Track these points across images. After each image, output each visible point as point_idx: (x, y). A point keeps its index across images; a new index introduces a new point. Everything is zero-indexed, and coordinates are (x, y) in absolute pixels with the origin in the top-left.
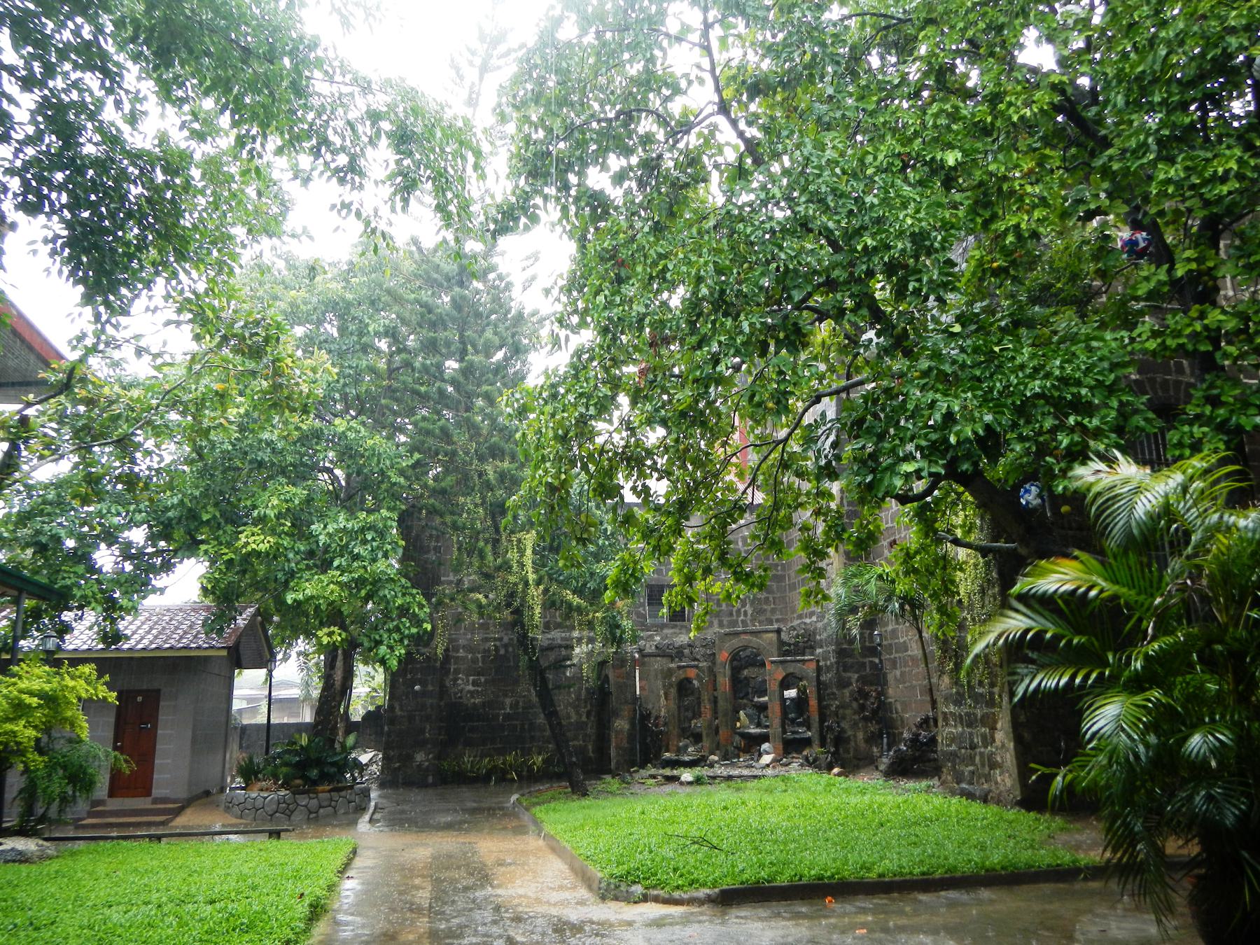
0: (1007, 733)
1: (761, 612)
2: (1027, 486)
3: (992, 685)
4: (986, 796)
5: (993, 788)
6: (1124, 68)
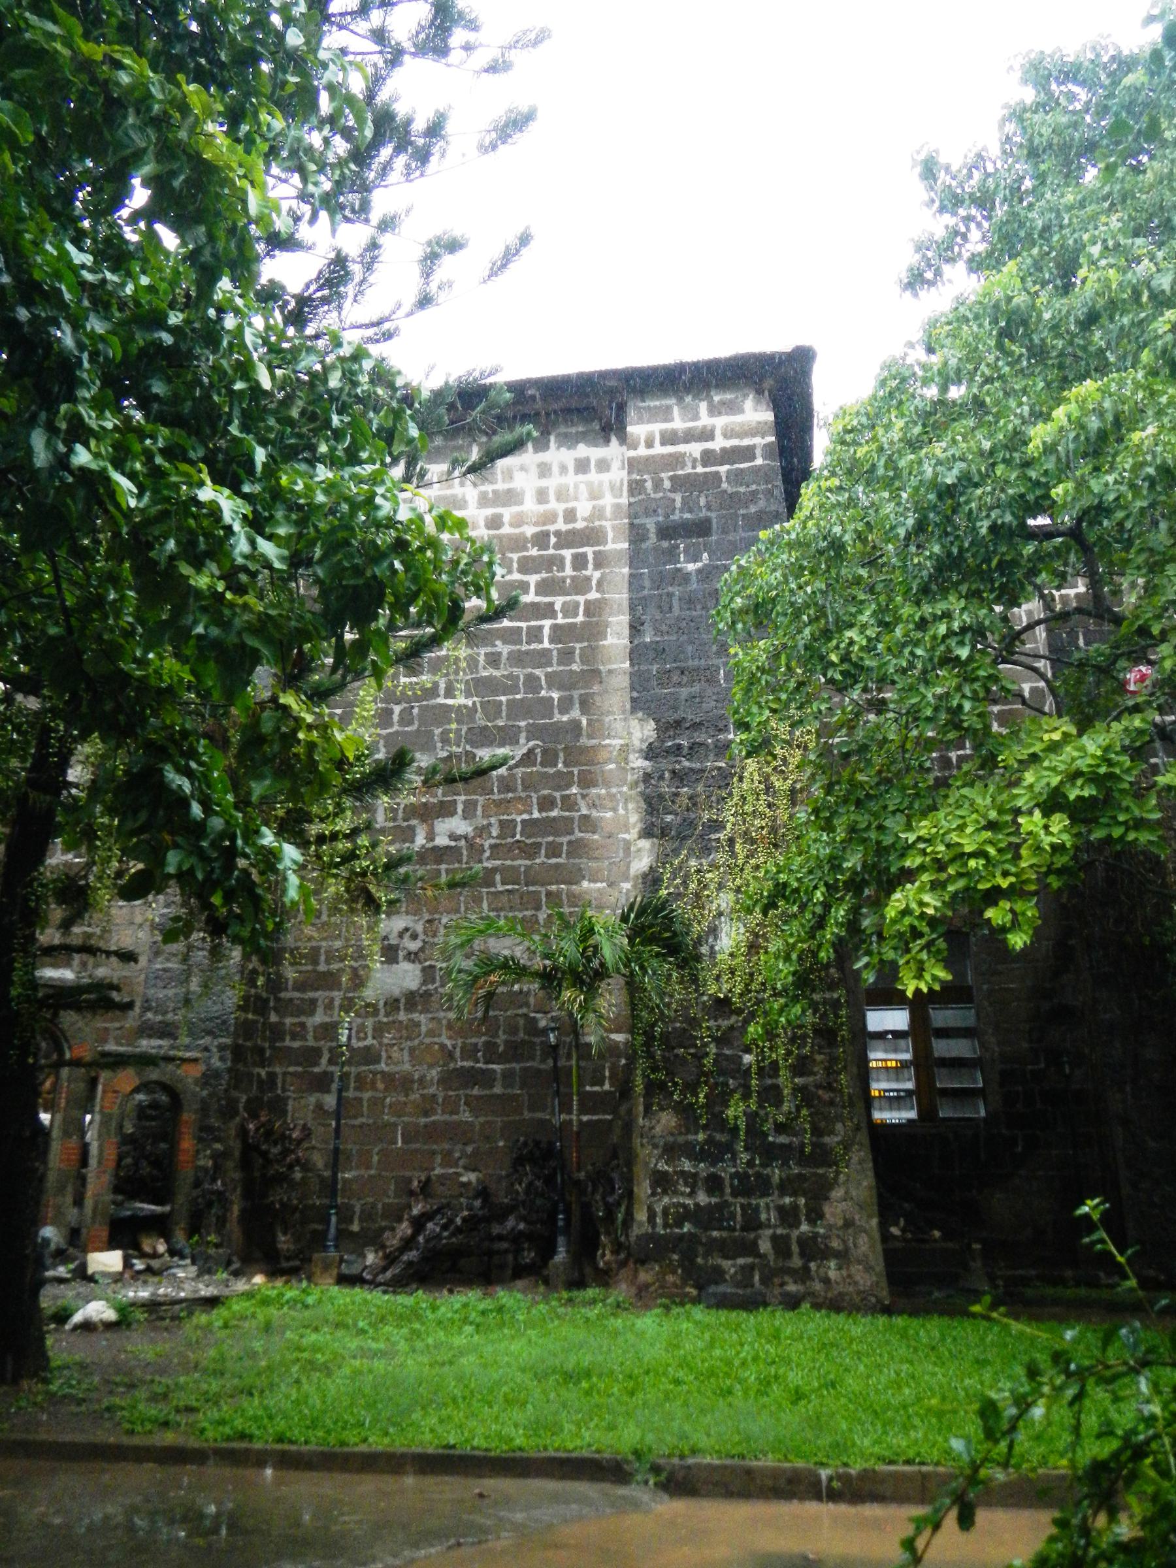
3: (817, 1131)
5: (818, 1286)
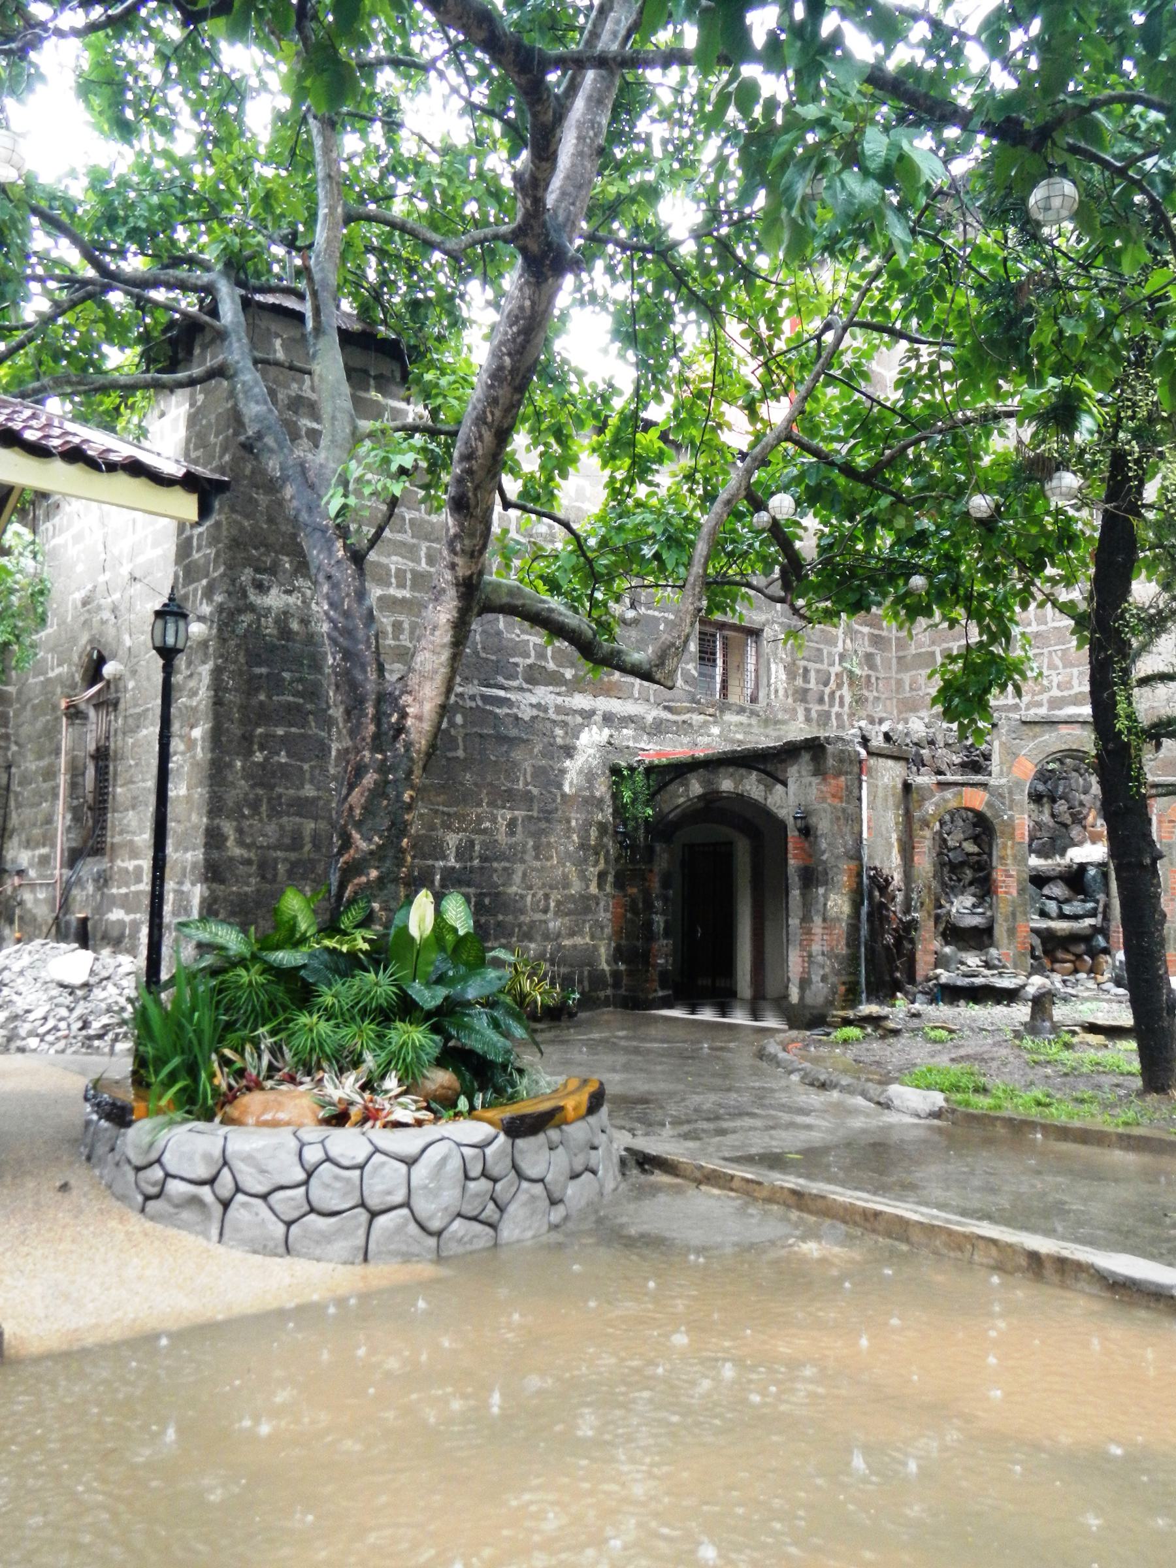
1: (859, 701)
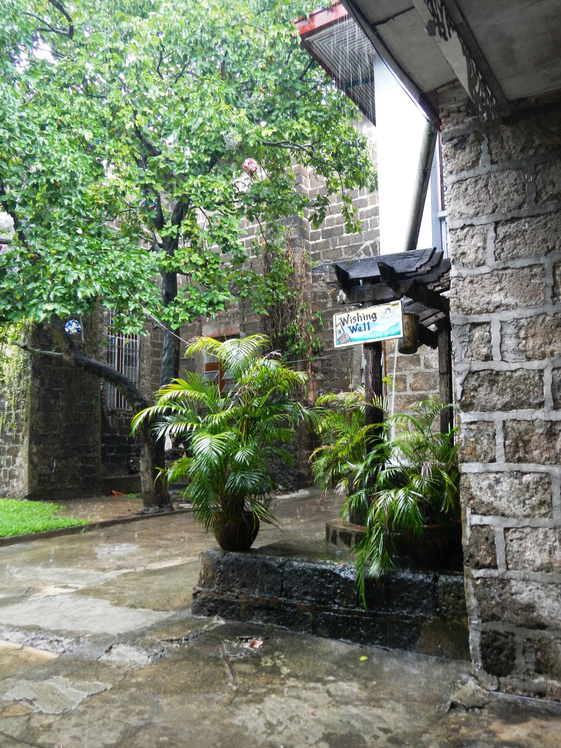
0: (24, 458)
2: (71, 322)
3: (18, 431)
4: (5, 494)
5: (11, 489)
6: (181, 120)
